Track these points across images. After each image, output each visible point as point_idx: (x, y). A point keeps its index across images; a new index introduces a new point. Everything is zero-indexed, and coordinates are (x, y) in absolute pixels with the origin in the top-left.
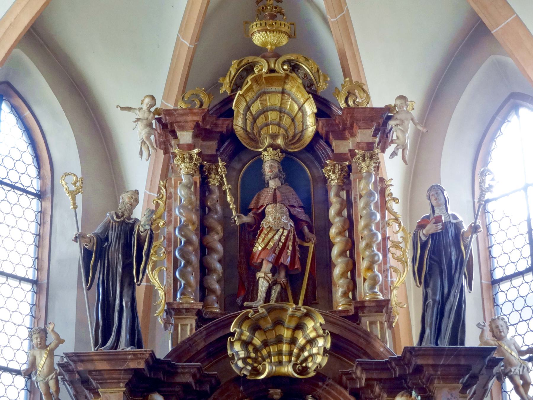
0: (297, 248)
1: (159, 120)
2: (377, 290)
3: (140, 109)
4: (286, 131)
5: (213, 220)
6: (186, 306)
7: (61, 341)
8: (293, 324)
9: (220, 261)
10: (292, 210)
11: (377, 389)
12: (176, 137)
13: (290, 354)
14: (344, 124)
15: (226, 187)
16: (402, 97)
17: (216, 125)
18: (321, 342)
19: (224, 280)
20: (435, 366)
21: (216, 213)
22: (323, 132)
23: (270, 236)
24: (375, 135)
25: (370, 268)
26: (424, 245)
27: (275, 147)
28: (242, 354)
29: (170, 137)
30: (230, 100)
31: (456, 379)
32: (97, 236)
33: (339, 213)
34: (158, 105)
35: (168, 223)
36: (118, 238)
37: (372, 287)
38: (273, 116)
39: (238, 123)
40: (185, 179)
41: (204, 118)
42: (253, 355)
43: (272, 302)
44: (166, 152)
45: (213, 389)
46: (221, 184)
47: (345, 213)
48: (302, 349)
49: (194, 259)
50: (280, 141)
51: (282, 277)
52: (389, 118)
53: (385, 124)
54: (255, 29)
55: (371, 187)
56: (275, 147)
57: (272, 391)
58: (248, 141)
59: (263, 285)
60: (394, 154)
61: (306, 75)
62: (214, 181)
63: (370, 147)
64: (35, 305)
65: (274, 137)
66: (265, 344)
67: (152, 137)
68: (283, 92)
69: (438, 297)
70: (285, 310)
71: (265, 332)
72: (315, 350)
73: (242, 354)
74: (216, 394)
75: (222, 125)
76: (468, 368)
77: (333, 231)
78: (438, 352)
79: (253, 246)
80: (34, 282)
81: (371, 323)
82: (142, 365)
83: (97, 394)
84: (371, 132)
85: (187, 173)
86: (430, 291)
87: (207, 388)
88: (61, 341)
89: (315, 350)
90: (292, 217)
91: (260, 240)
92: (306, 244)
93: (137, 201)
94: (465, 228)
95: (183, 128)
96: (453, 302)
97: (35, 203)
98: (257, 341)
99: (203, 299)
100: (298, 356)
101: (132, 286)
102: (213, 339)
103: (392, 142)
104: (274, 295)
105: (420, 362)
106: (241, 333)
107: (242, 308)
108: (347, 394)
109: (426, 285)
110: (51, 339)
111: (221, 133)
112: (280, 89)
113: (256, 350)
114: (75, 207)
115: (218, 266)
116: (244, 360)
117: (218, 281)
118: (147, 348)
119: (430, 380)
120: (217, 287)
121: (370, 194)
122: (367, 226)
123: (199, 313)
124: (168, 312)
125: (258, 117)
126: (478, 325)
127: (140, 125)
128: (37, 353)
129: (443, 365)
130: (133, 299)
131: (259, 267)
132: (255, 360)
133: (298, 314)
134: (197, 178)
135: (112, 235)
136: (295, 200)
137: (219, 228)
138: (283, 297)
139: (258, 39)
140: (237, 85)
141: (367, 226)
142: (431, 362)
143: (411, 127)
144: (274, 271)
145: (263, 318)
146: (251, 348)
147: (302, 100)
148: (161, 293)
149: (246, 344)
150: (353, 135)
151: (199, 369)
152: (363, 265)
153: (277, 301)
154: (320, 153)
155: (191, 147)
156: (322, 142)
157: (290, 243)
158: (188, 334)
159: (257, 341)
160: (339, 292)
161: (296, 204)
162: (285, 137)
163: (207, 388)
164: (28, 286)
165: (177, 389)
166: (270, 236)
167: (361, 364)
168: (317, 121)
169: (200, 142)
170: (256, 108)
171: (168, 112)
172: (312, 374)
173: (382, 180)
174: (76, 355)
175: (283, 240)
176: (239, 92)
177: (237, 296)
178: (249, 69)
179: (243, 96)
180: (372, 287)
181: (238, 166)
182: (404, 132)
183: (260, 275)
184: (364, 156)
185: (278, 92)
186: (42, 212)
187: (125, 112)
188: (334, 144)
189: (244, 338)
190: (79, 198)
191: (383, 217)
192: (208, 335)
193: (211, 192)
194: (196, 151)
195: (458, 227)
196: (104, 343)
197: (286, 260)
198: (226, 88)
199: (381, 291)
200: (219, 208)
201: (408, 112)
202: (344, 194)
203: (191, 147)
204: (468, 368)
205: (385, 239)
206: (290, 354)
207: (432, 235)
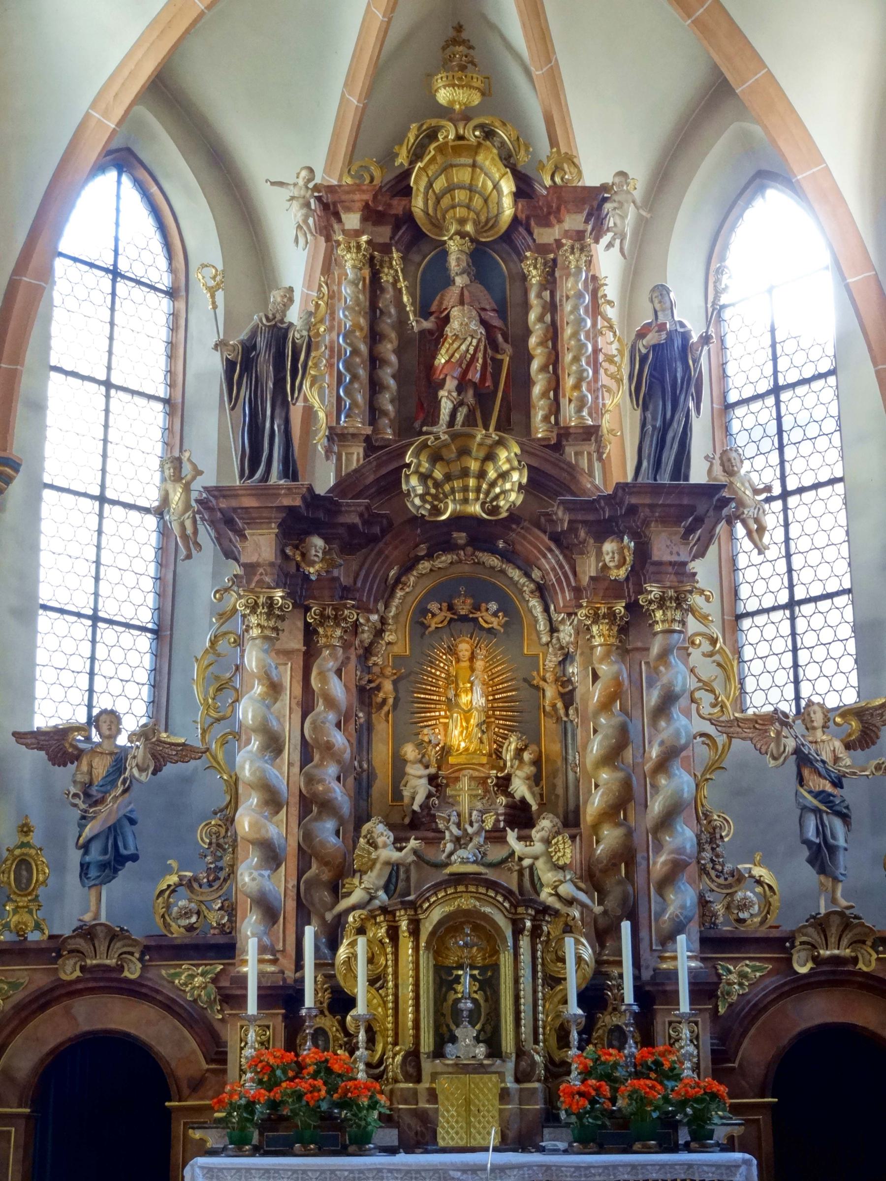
0: (489, 361)
1: (319, 199)
2: (585, 413)
3: (295, 185)
4: (478, 214)
5: (387, 325)
6: (351, 431)
7: (198, 473)
8: (482, 455)
9: (394, 377)
10: (483, 314)
11: (582, 534)
12: (340, 220)
13: (478, 490)
14: (550, 207)
15: (402, 284)
16: (622, 174)
17: (390, 206)
18: (515, 476)
19: (400, 400)
20: (652, 507)
21: (390, 316)
22: (522, 216)
23: (455, 346)
24: (587, 221)
25: (577, 387)
26: (643, 359)
27: (462, 235)
28: (420, 490)
29: (333, 220)
30: (407, 174)
31: (678, 521)
32: (242, 343)
33: (541, 319)
34: (318, 180)
35: (330, 329)
36: (269, 346)
37: (579, 410)
38: (461, 196)
39: (418, 204)
40: (351, 274)
41: (375, 197)
42: (433, 491)
43: (458, 427)
44: (328, 239)
45: (384, 532)
46: (396, 281)
47: (548, 318)
48: (493, 484)
49: (362, 373)
50: (469, 228)
51: (470, 397)
52: (605, 200)
53: (600, 207)
54: (440, 83)
55: (580, 286)
57: (455, 535)
58: (430, 227)
60: (610, 245)
61: (503, 143)
62: (386, 278)
63: (579, 236)
64: (168, 430)
65: (462, 222)
66: (448, 477)
67: (311, 221)
68: (474, 165)
69: (659, 423)
70: (473, 437)
71: (448, 463)
72: (508, 486)
73: (420, 490)
74: (388, 537)
75: (397, 206)
76: (692, 509)
77: (533, 341)
78: (656, 490)
79: (434, 357)
80: (167, 402)
81: (576, 454)
82: (298, 502)
83: (243, 537)
84: (582, 217)
85: (354, 267)
86: (649, 415)
87: (377, 530)
88: (198, 473)
89: (508, 486)
90: (483, 322)
91: (443, 351)
92: (499, 357)
93: (291, 300)
94: (695, 338)
95: (348, 210)
96: (677, 428)
97: (165, 303)
98: (438, 475)
99: (373, 421)
100: (487, 493)
101: (286, 405)
102: (384, 471)
103: (608, 230)
104: (460, 418)
105: (634, 500)
106: (419, 465)
107: (421, 433)
108: (546, 539)
109: (645, 408)
110: (187, 469)
111: (396, 216)
112: (470, 161)
113: (437, 485)
114: (215, 307)
115: (392, 383)
116: (422, 497)
117: (392, 401)
118: (304, 482)
119: (646, 523)
120: (390, 408)
121: (580, 295)
122: (575, 334)
123: (368, 439)
124: (330, 438)
125: (442, 197)
126: (707, 458)
127: (296, 205)
128: (170, 486)
129: (663, 505)
130: (287, 422)
131: (441, 384)
132: (435, 497)
133: (489, 442)
134: (366, 272)
135: (261, 342)
136: (487, 302)
137: (393, 335)
138: (470, 421)
139: (444, 96)
140: (417, 155)
141: (575, 334)
142: (648, 501)
143: (631, 211)
144: (460, 389)
145: (445, 445)
146: (430, 483)
147: (497, 176)
148: (322, 415)
149: (424, 478)
150: (560, 221)
151: (368, 507)
152: (569, 382)
153: (463, 425)
154: (519, 242)
155: (358, 233)
156: (521, 230)
157: (480, 355)
158: (354, 465)
159: (438, 475)
160: (538, 416)
161: (488, 307)
162: (476, 223)
163: (377, 530)
164: (159, 406)
165: (341, 531)
166: (455, 346)
167: (562, 502)
168: (515, 203)
169: (369, 227)
170: (440, 184)
171: (330, 189)
172: (504, 515)
173: (594, 278)
174: (217, 488)
175: (471, 351)
176: (420, 164)
177: (416, 419)
178: (432, 135)
179: (424, 169)
180: (579, 410)
181: (416, 258)
182: (623, 218)
183: (442, 393)
184: (572, 248)
185: (469, 166)
186: (174, 315)
187: (275, 188)
188: (537, 231)
189: (422, 470)
190: (220, 295)
191: (594, 324)
192: (379, 466)
193: (383, 290)
194: (365, 238)
195: (686, 336)
196: (252, 473)
197: (475, 376)
198: (402, 159)
199: (590, 414)
200: (393, 311)
201: (628, 192)
202: (547, 295)
203: (358, 233)
204: (692, 509)
205: (596, 351)
206: (478, 490)
207: (654, 347)
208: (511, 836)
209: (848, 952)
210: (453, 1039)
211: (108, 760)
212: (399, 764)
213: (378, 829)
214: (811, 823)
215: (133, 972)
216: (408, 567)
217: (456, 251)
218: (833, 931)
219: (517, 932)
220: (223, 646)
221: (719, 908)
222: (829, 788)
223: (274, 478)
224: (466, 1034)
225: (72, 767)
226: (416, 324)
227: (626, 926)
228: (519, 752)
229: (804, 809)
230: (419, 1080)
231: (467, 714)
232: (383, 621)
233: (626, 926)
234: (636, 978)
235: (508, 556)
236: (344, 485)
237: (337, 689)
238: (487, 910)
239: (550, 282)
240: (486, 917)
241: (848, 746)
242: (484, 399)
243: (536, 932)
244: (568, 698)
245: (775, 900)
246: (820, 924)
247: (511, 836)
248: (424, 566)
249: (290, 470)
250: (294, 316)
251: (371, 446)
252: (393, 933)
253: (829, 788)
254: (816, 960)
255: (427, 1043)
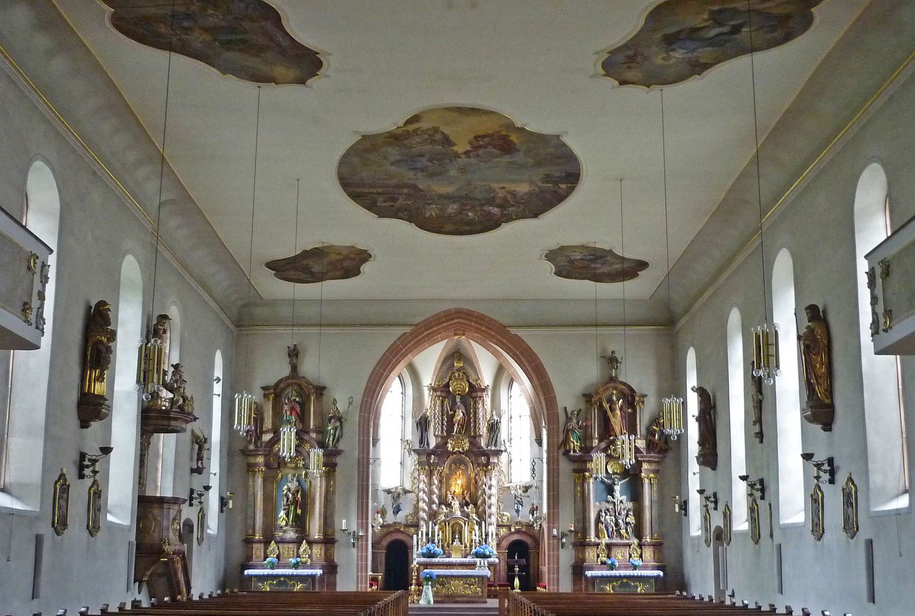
27: (459, 394)
28: (450, 446)
33: (473, 411)
49: (440, 423)
50: (460, 393)
56: (459, 394)
59: (455, 429)
77: (471, 416)
78: (491, 450)
90: (462, 412)
98: (454, 443)
131: (454, 425)
138: (460, 432)
144: (458, 425)
149: (451, 444)
186: (403, 397)
197: (461, 423)
208: (465, 507)
209: (521, 527)
210: (455, 541)
211: (397, 493)
212: (446, 495)
213: (443, 507)
214: (516, 505)
215: (402, 529)
216: (448, 458)
217: (458, 399)
218: (518, 525)
219: (465, 525)
220: (415, 471)
221: (500, 520)
222: (519, 499)
223: (426, 445)
224: (457, 540)
225: (391, 494)
226: (450, 413)
227: (483, 522)
228: (467, 493)
229: (515, 503)
230: (449, 547)
231: (458, 485)
232: (444, 467)
233: (483, 522)
234: (485, 531)
235: (466, 456)
236: (437, 446)
237: (436, 482)
238: (460, 522)
239: (475, 403)
240: (460, 523)
241: (523, 492)
242: (462, 426)
243: (468, 524)
244: (476, 482)
245: (509, 519)
246: (516, 523)
247: (465, 507)
248: (451, 457)
249: (428, 444)
250: (428, 414)
251: (442, 437)
252: (445, 524)
253: (519, 499)
254: (515, 529)
255: (450, 542)
